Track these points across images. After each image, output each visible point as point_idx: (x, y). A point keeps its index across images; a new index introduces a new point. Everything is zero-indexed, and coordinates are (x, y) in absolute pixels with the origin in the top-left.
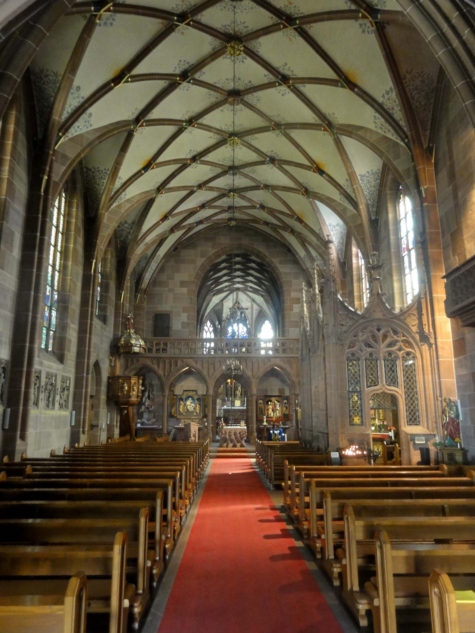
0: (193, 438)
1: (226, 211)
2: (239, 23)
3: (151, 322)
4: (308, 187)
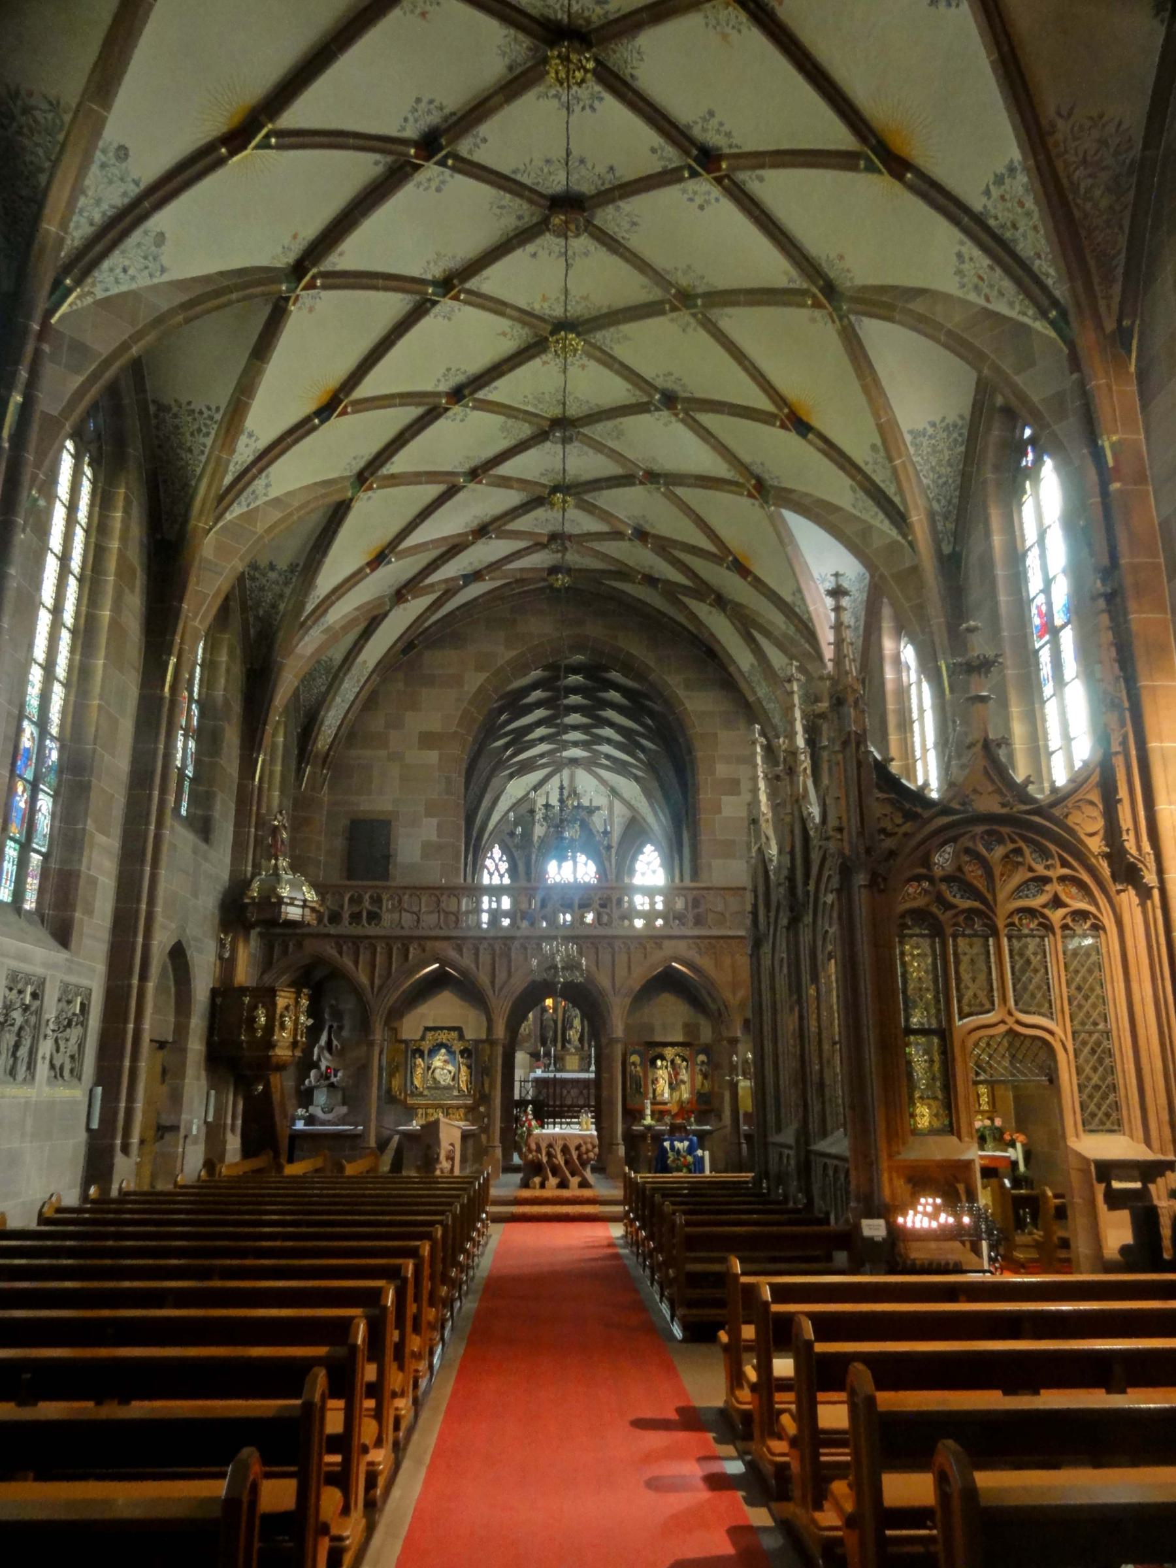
0: (445, 1164)
1: (544, 546)
3: (339, 843)
4: (766, 476)
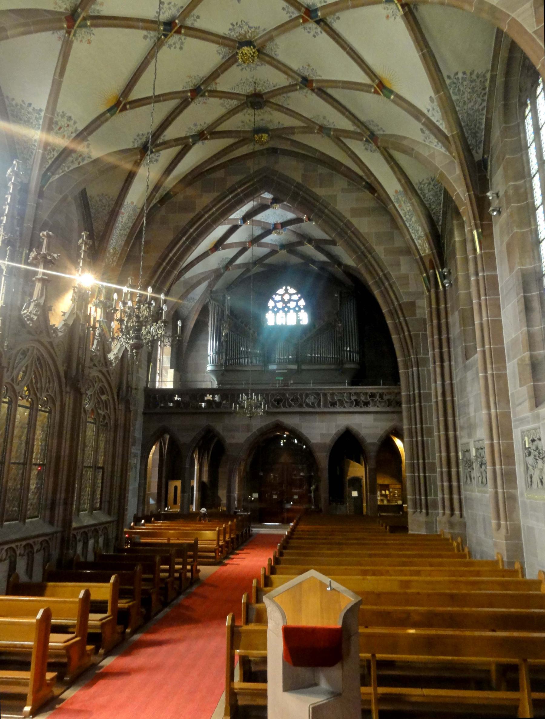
2: (247, 68)
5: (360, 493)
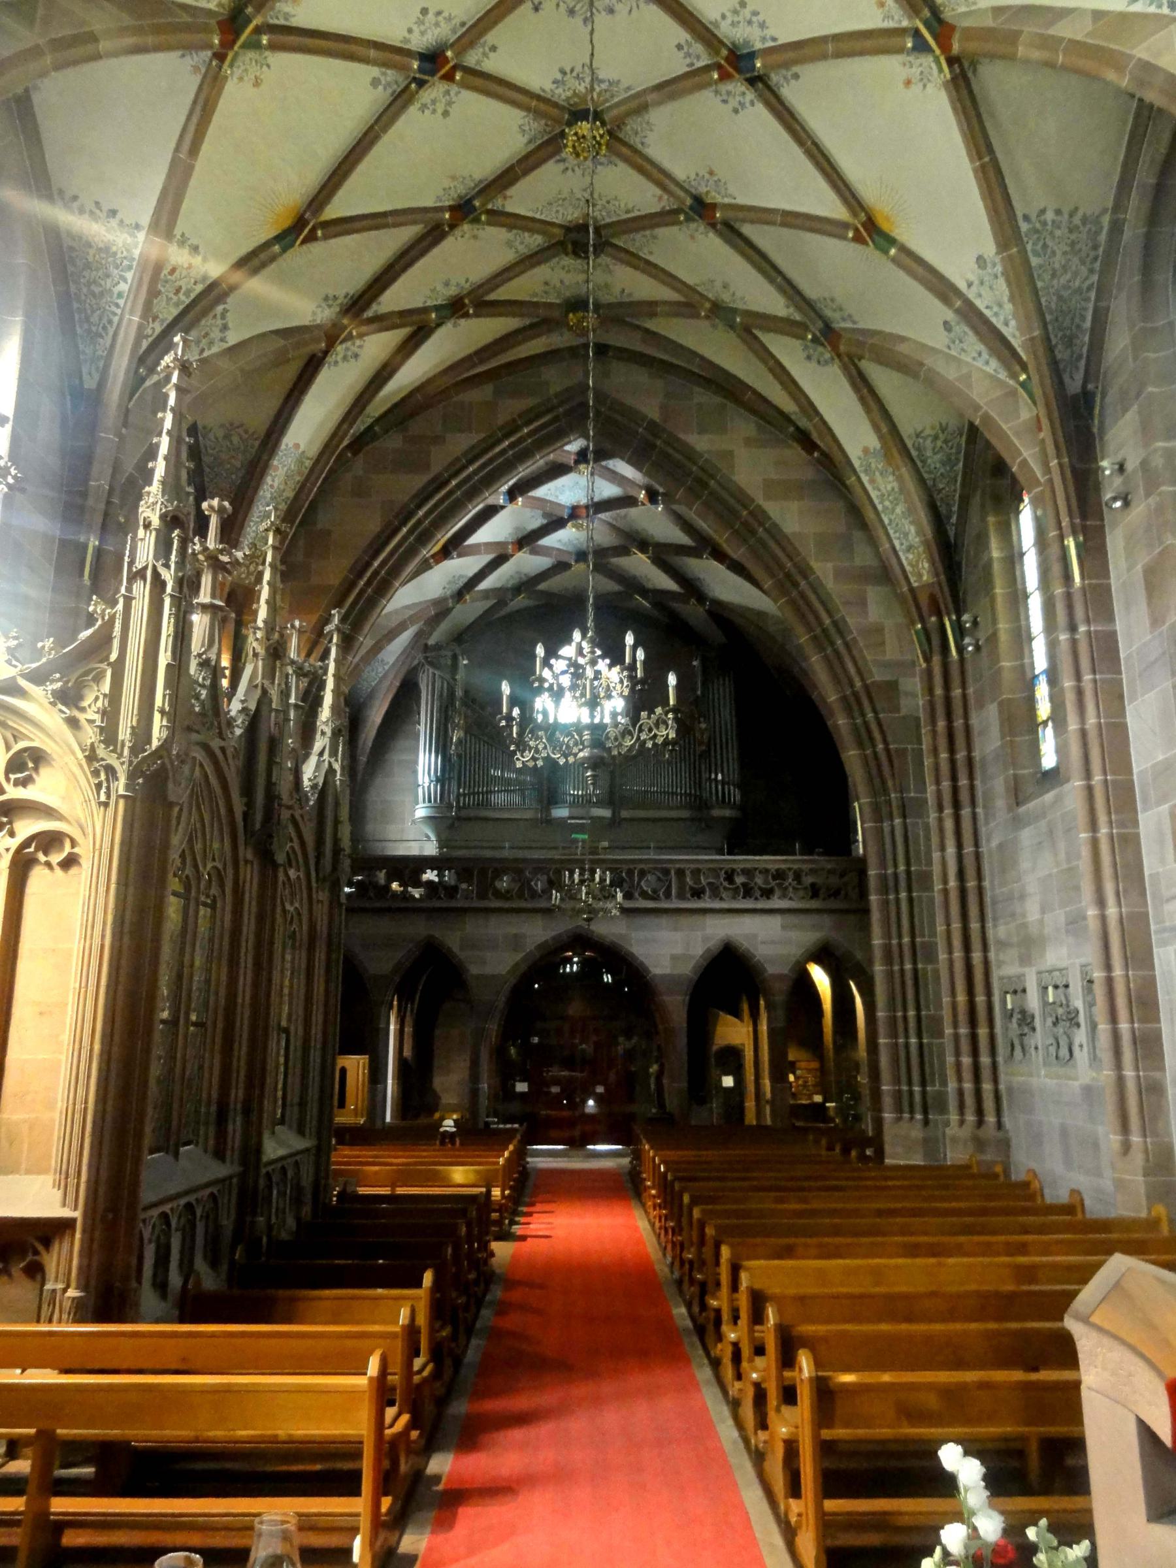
2: (576, 168)
5: (739, 1081)
